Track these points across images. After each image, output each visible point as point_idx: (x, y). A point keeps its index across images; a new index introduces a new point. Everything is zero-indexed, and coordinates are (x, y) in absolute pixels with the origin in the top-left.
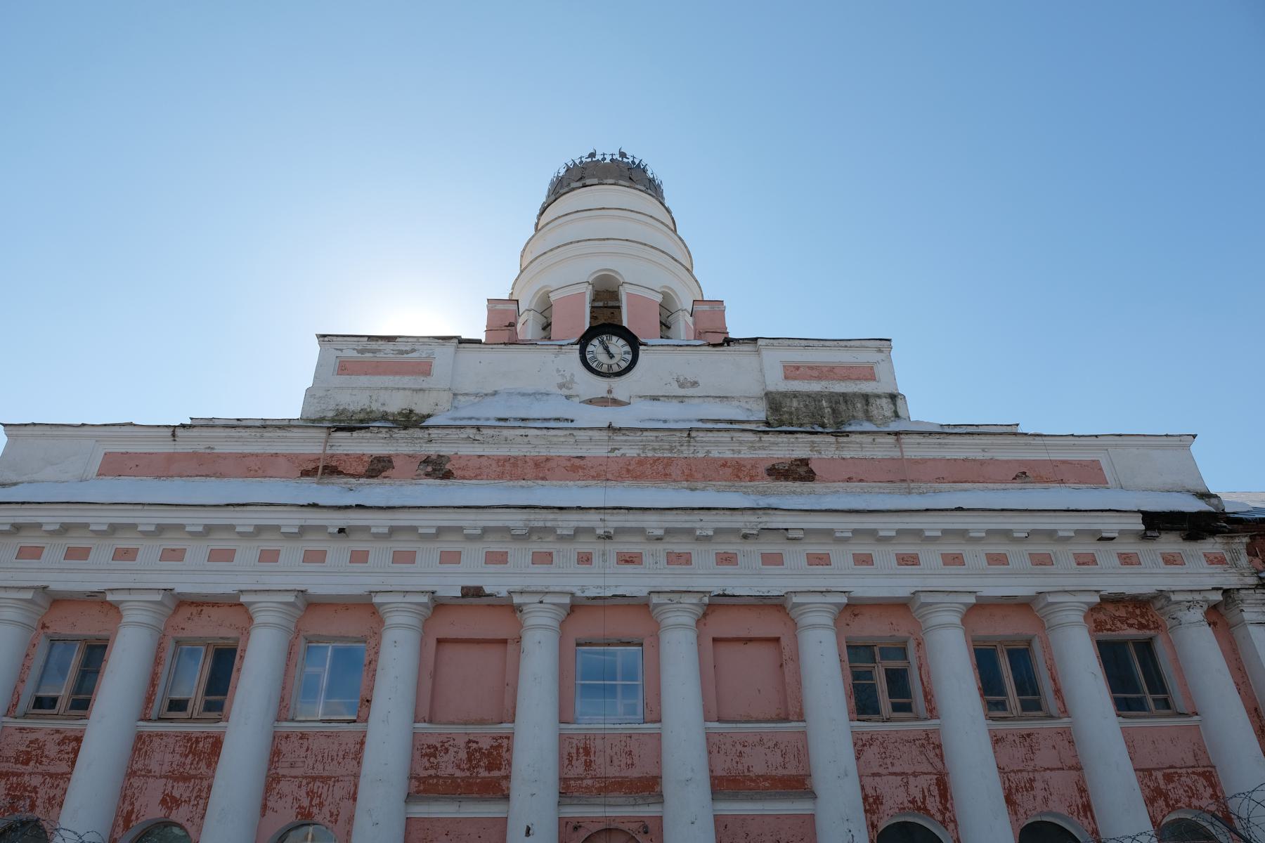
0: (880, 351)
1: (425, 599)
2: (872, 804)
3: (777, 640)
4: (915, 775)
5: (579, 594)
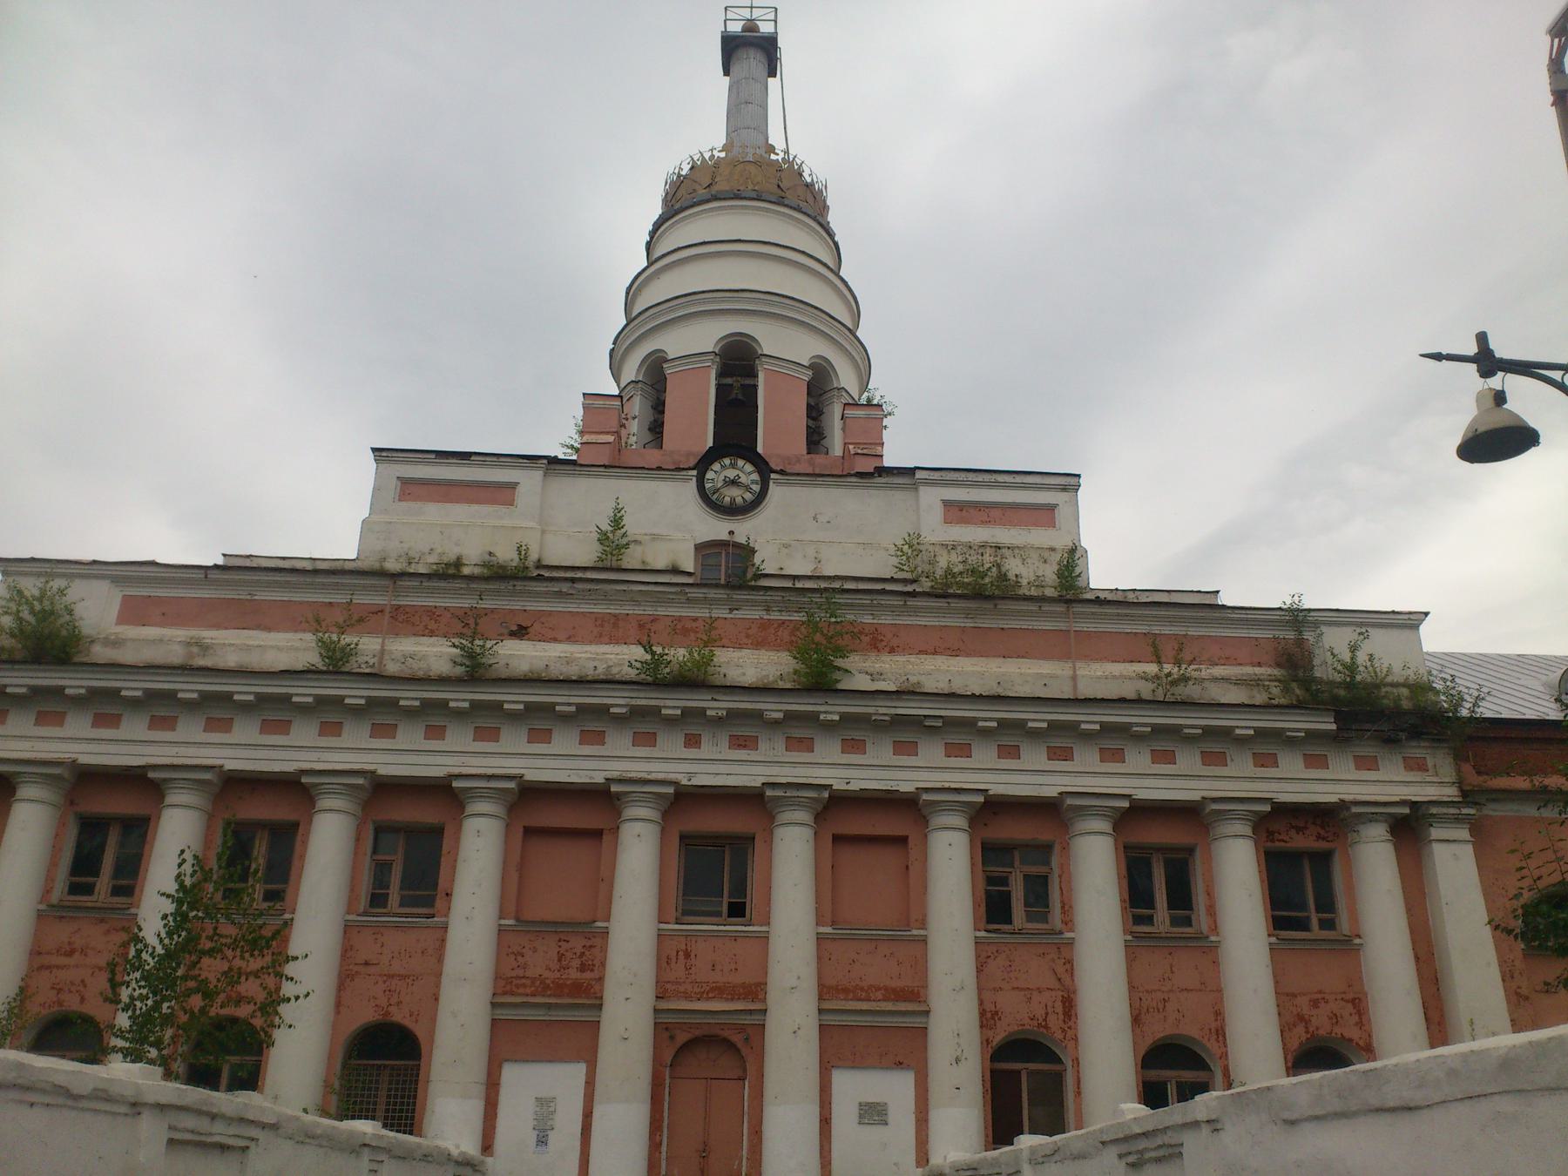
0: (1064, 489)
2: (987, 1018)
4: (1039, 990)
5: (685, 782)
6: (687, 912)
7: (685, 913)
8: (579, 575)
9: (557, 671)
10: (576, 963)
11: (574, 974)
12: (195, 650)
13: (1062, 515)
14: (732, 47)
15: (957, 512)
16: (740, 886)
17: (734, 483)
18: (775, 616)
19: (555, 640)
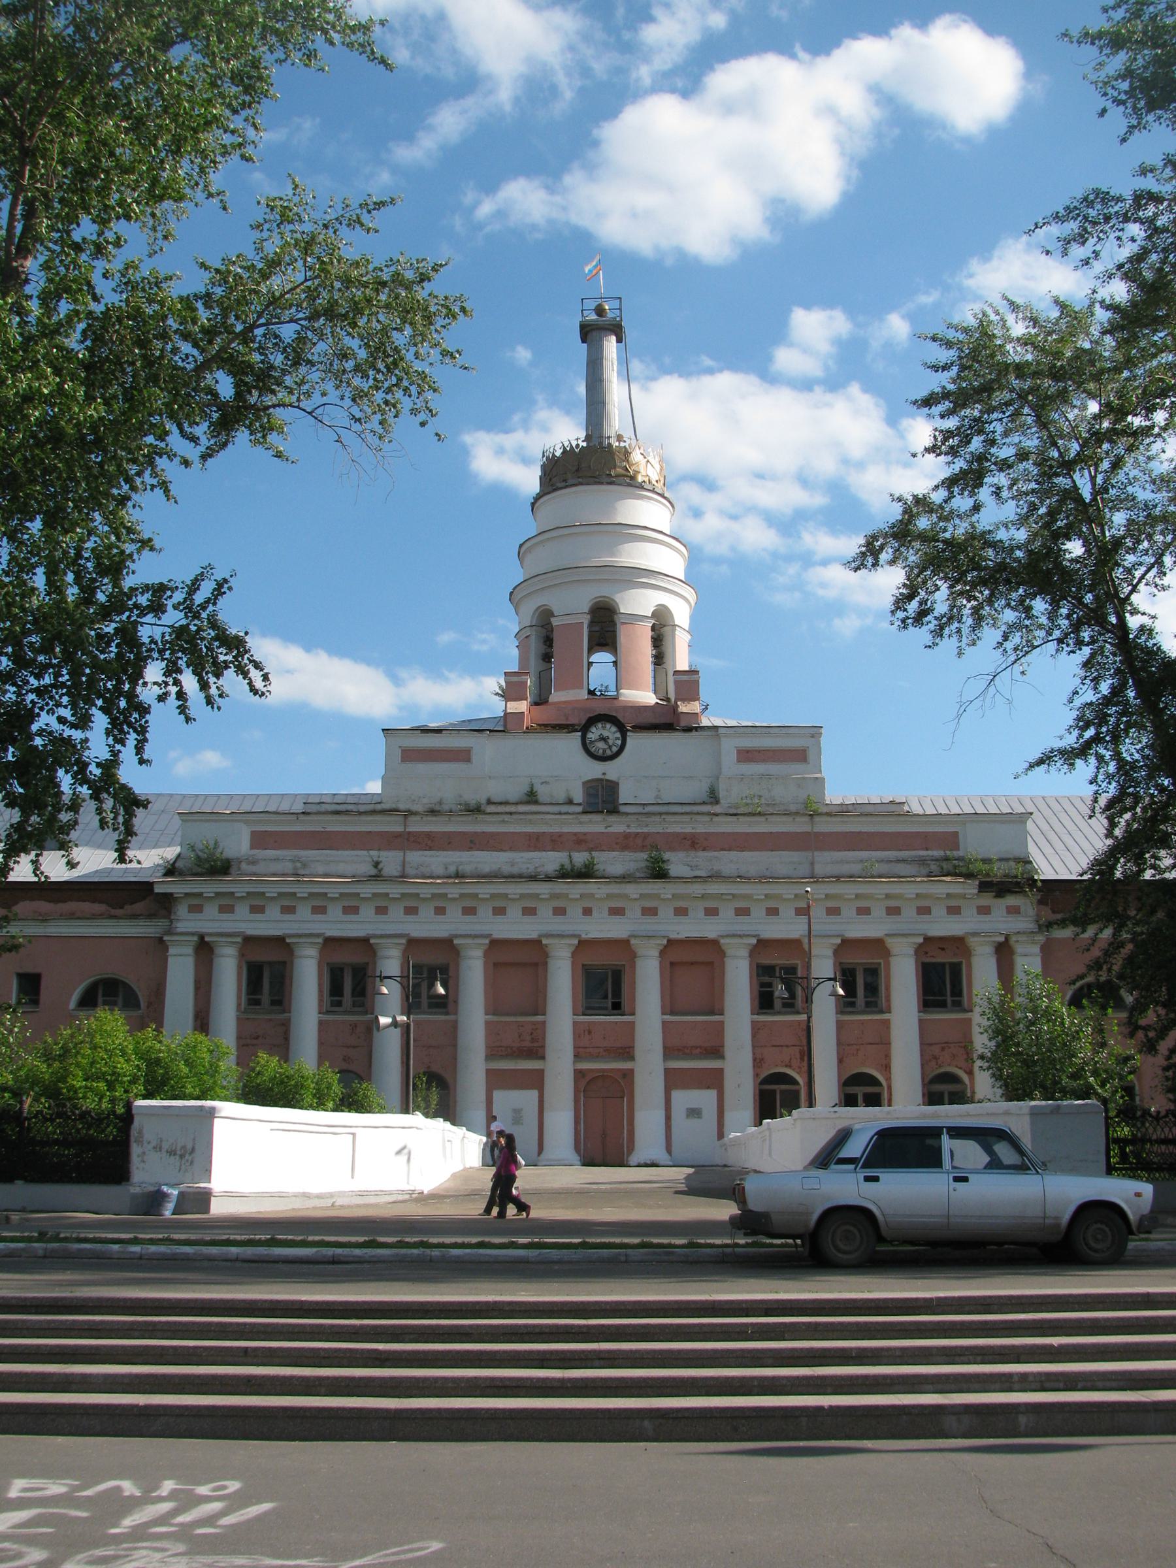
1: (487, 941)
2: (758, 1062)
3: (711, 963)
5: (584, 936)
6: (589, 1010)
7: (587, 1008)
8: (513, 809)
9: (507, 869)
10: (529, 1038)
11: (527, 1044)
12: (299, 865)
13: (811, 756)
15: (746, 755)
16: (617, 991)
17: (603, 739)
18: (633, 830)
19: (502, 850)
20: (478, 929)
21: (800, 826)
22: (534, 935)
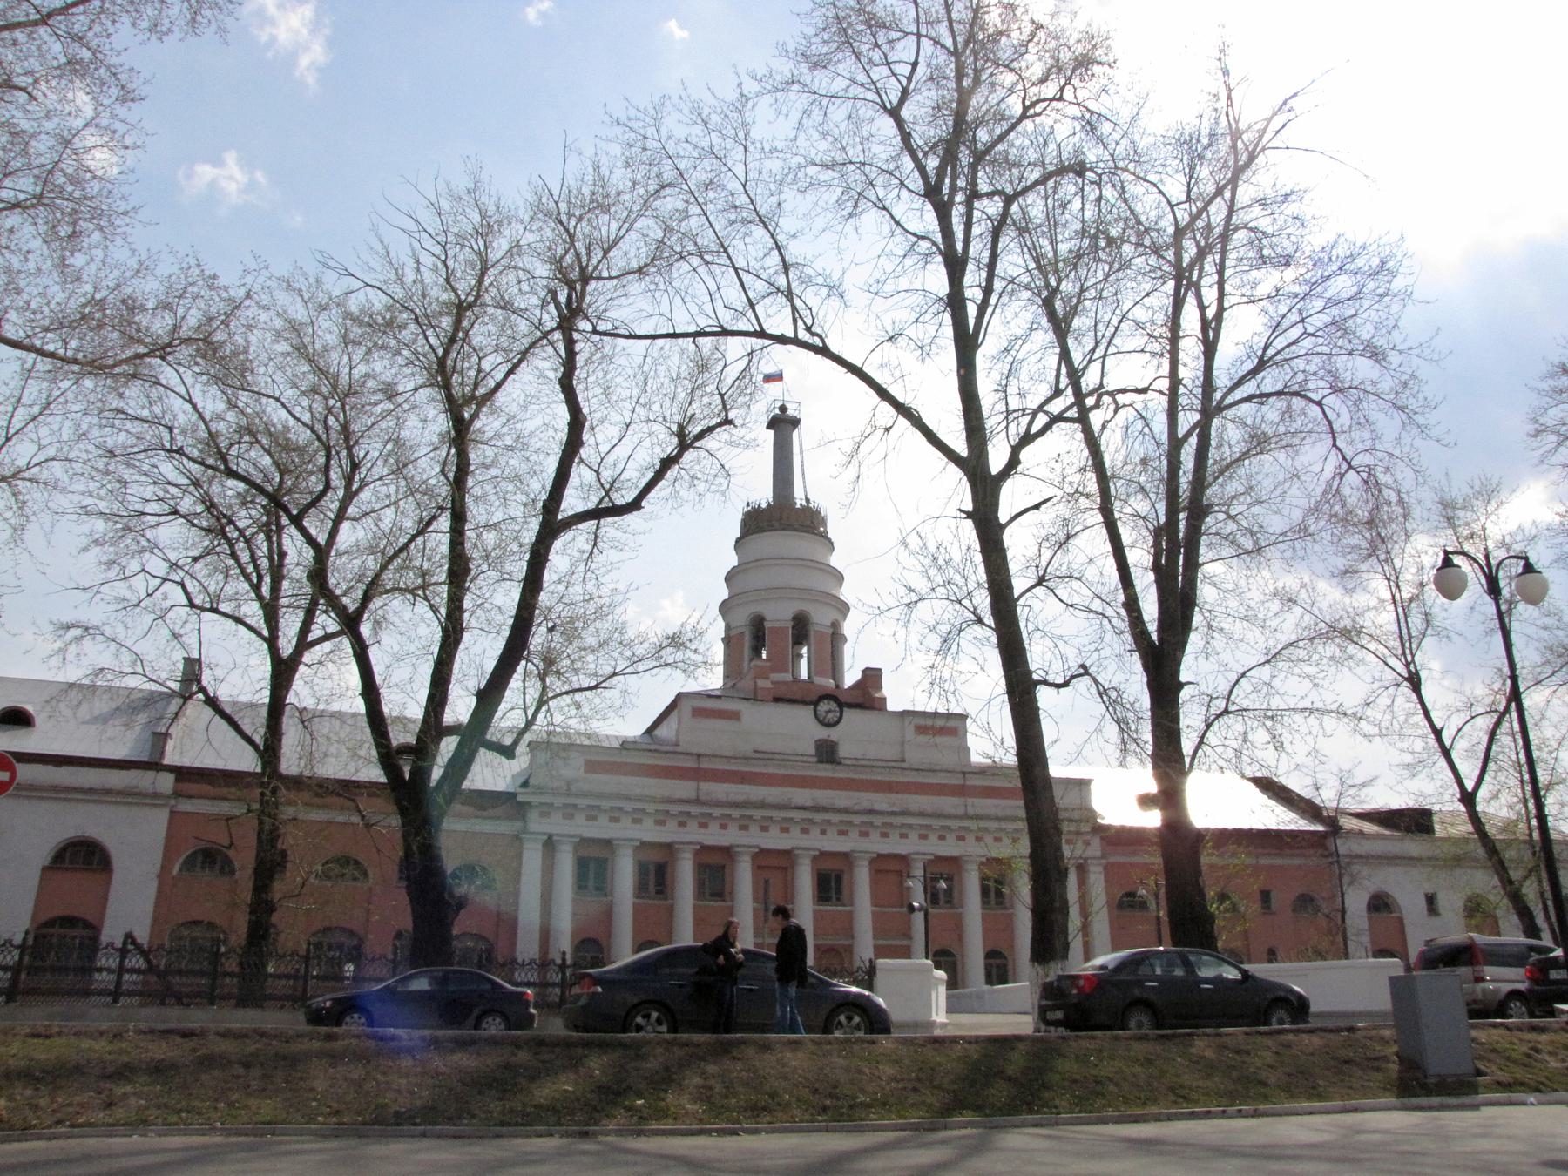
14: (773, 424)
16: (839, 891)
20: (688, 838)
21: (956, 780)
22: (788, 847)
